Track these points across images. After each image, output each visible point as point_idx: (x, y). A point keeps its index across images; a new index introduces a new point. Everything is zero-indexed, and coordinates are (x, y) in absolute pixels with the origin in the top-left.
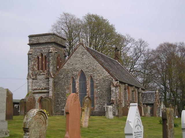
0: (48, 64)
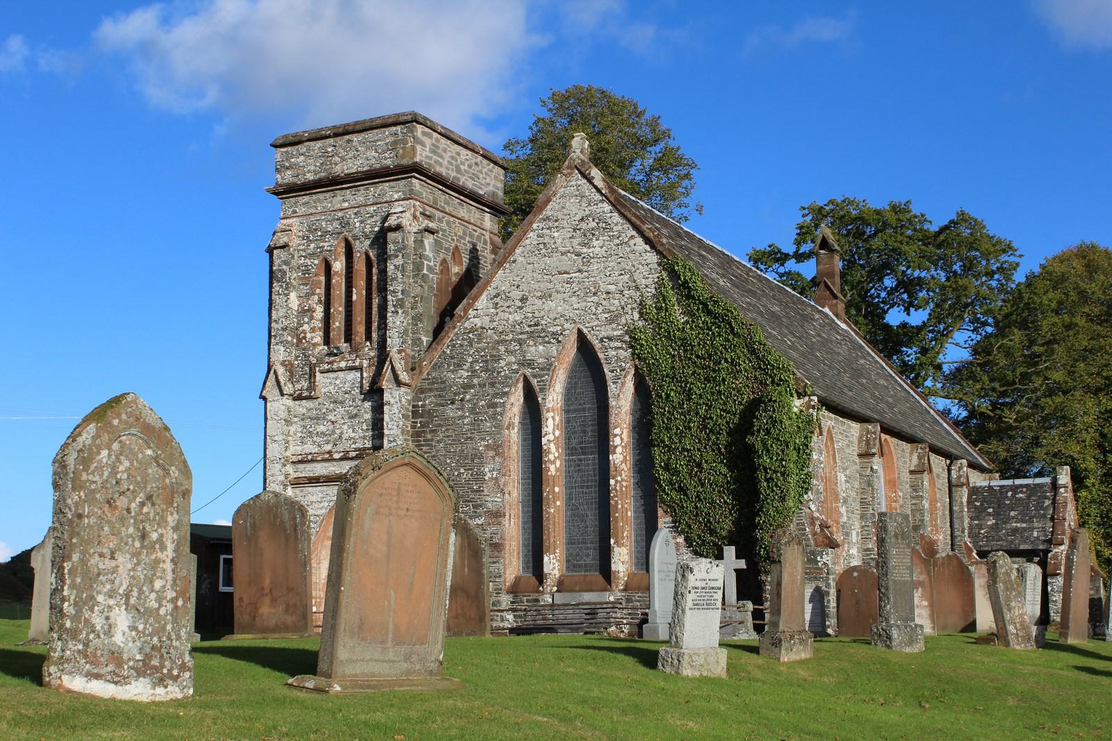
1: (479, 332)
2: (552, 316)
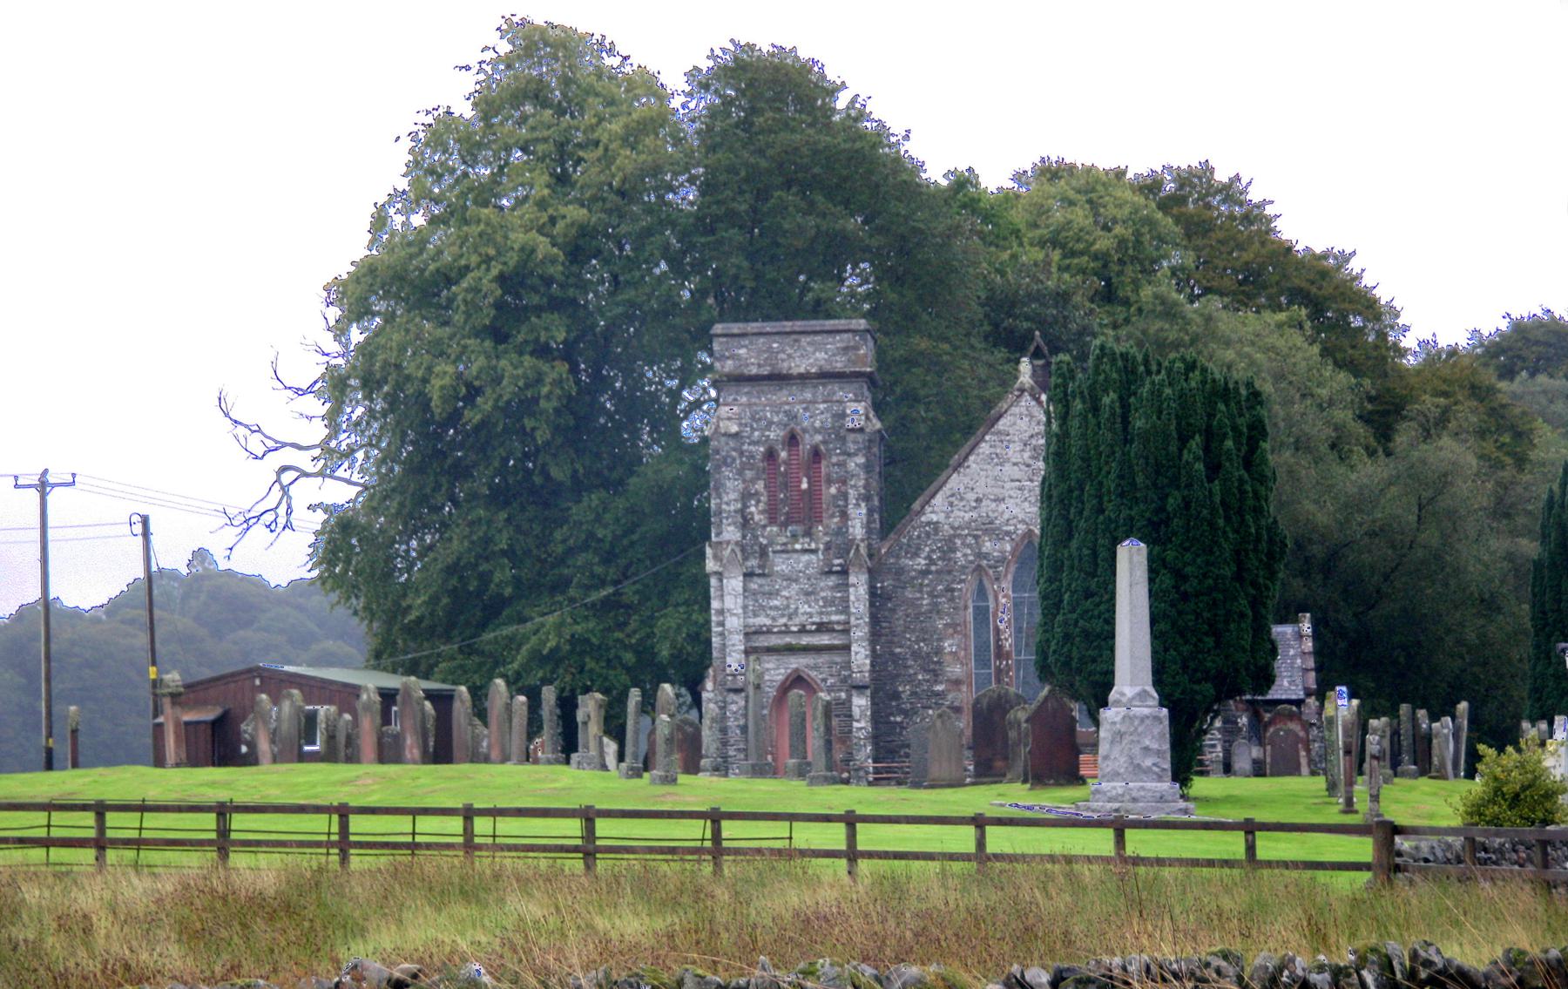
0: (833, 490)
1: (936, 525)
2: (1006, 516)
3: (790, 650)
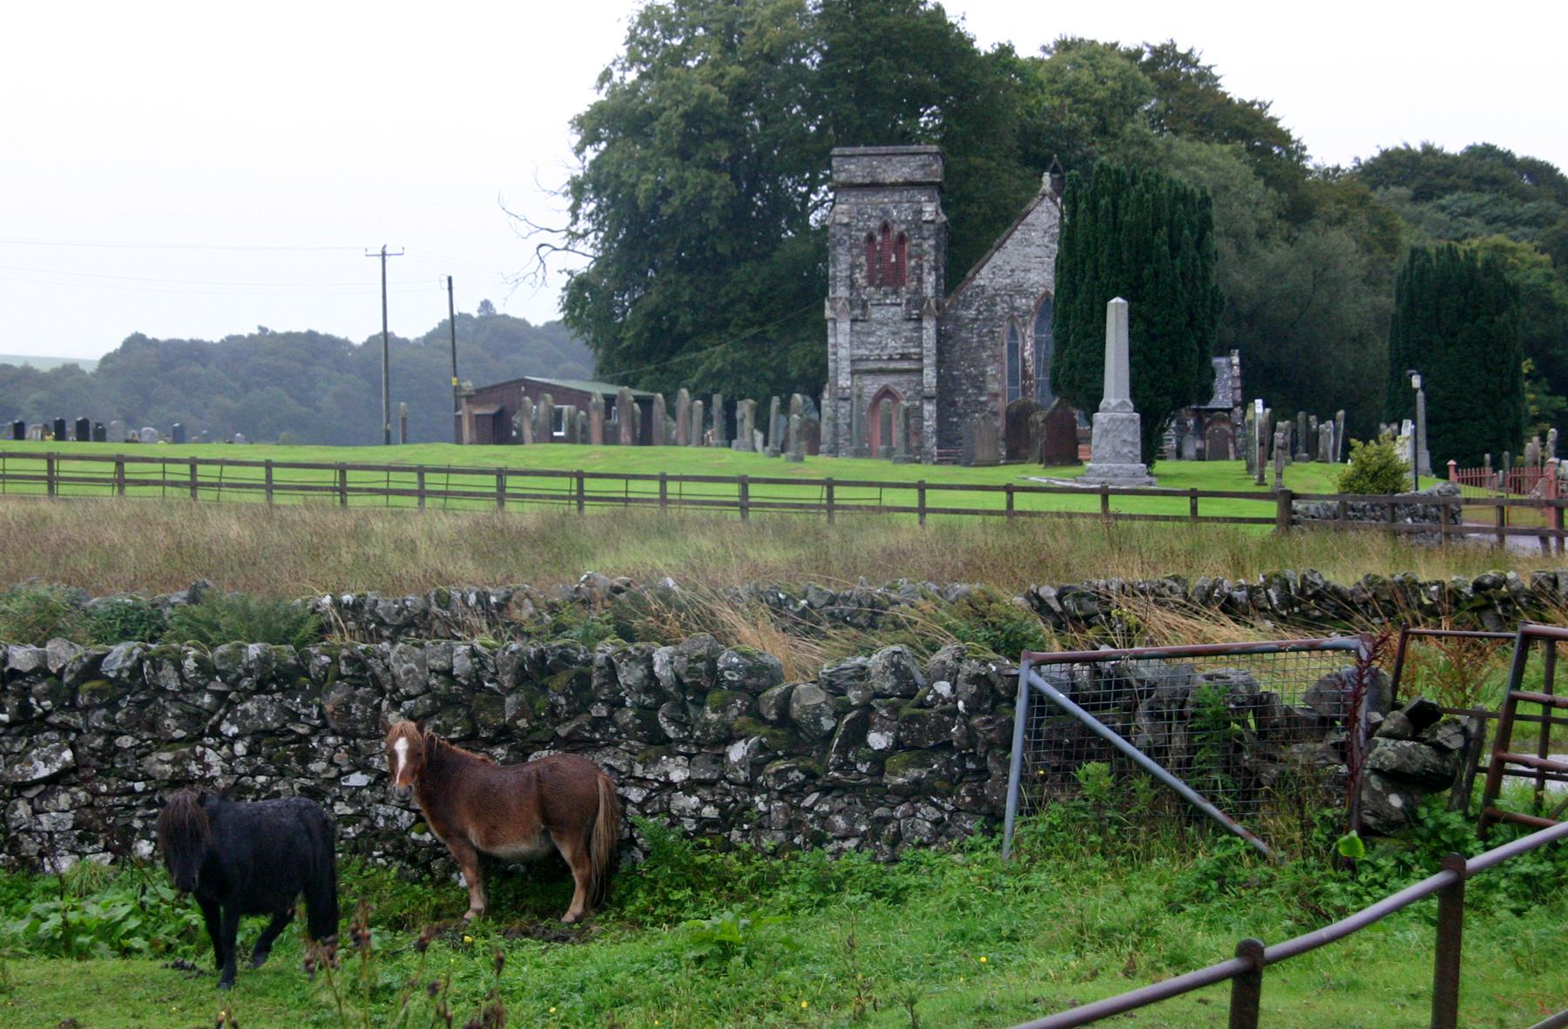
0: (913, 263)
3: (882, 372)
